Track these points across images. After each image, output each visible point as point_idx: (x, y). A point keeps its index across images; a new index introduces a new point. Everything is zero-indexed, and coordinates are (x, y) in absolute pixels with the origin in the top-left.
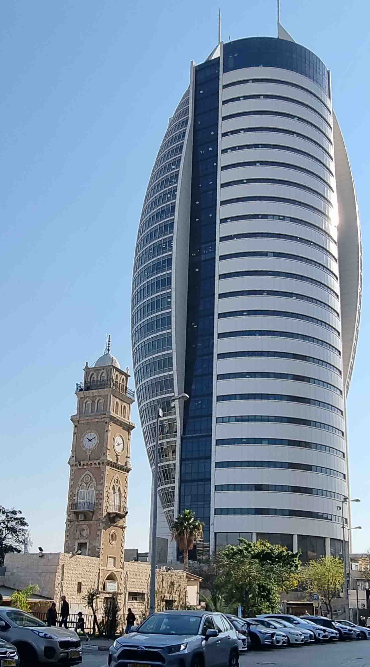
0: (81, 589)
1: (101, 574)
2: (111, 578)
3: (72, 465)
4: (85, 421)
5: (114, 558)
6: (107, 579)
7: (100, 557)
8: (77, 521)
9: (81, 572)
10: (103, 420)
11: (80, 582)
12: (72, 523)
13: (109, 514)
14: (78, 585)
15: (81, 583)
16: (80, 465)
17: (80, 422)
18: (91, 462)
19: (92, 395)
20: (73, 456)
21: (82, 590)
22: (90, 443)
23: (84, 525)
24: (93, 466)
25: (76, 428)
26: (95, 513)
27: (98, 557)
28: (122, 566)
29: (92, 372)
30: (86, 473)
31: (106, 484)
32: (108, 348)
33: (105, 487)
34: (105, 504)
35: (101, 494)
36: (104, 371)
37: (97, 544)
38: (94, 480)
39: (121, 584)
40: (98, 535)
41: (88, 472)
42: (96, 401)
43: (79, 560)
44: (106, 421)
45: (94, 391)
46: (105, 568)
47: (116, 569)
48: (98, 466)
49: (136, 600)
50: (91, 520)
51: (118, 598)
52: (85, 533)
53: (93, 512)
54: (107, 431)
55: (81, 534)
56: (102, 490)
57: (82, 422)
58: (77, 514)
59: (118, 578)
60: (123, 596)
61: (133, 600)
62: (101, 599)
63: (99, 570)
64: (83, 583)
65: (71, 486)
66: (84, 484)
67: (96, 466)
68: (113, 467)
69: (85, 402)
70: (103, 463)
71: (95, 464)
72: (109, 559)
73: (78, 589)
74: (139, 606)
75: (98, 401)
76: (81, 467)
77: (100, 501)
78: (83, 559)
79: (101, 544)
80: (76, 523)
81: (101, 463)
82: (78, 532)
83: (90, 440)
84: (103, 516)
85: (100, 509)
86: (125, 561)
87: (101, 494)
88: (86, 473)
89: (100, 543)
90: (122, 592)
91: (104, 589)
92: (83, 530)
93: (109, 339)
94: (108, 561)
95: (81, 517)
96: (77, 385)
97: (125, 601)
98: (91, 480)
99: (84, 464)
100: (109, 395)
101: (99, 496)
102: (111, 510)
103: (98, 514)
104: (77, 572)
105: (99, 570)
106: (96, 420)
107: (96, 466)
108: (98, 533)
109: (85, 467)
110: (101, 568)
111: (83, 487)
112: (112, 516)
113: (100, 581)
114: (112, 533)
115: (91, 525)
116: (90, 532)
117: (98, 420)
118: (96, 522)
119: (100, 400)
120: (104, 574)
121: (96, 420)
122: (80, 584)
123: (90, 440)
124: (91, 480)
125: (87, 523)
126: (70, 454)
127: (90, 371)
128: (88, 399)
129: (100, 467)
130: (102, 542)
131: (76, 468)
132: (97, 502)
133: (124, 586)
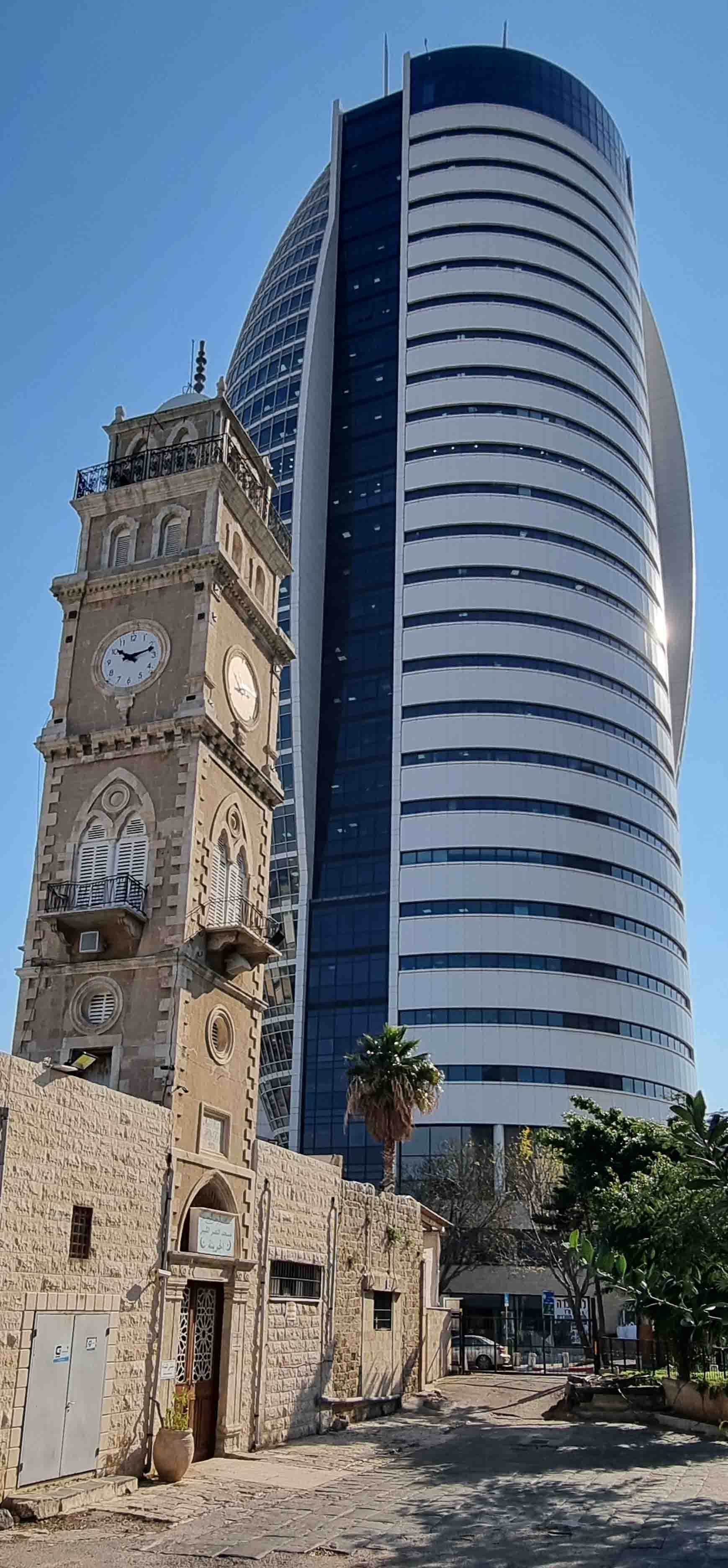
0: (87, 1240)
1: (177, 1180)
2: (212, 1198)
3: (53, 753)
4: (109, 595)
5: (224, 1120)
6: (195, 1203)
7: (175, 1104)
8: (72, 963)
9: (90, 1160)
10: (185, 578)
11: (87, 1204)
12: (48, 973)
13: (207, 935)
14: (75, 1219)
15: (89, 1211)
16: (87, 750)
17: (90, 599)
18: (136, 734)
19: (138, 503)
20: (60, 721)
21: (94, 1242)
22: (129, 665)
23: (102, 976)
24: (145, 748)
25: (73, 624)
26: (150, 926)
27: (164, 1101)
28: (248, 1157)
29: (138, 436)
30: (112, 776)
31: (198, 813)
32: (194, 382)
33: (195, 824)
34: (193, 891)
35: (178, 848)
36: (189, 424)
37: (160, 1052)
38: (146, 798)
39: (247, 1227)
40: (166, 1013)
41: (120, 772)
42: (157, 522)
43: (80, 1099)
44: (198, 581)
45: (149, 484)
46: (192, 1156)
47: (230, 1167)
48: (165, 745)
49: (293, 1293)
50: (134, 956)
51: (238, 1285)
52: (102, 1011)
53: (141, 924)
54: (201, 616)
55: (84, 1014)
56: (182, 834)
57: (99, 597)
58: (69, 931)
59: (238, 1201)
60: (252, 1276)
61: (281, 1293)
62: (175, 1287)
63: (169, 1159)
64: (97, 1213)
65: (47, 831)
66: (103, 822)
67: (156, 748)
68: (224, 757)
69: (111, 528)
70: (186, 732)
71: (152, 738)
72: (203, 1118)
73: (73, 1238)
74: (303, 1318)
75: (165, 522)
76: (91, 758)
77: (173, 879)
78: (102, 1101)
79: (178, 1053)
80: (67, 971)
81: (178, 731)
82: (74, 1009)
83: (132, 658)
84: (187, 938)
85: (173, 907)
86: (257, 1137)
87: (178, 848)
88: (112, 776)
89: (173, 1042)
90: (249, 1259)
91: (185, 1247)
92: (96, 998)
93: (202, 353)
94: (203, 1127)
95: (89, 943)
96: (80, 476)
97: (261, 1296)
98: (134, 799)
99: (101, 746)
100: (211, 494)
101: (170, 857)
102: (214, 920)
103: (163, 932)
104: (72, 1159)
105: (169, 1159)
106: (157, 584)
107: (156, 748)
108: (165, 1004)
109: (109, 755)
110: (177, 1153)
111: (98, 833)
112: (218, 945)
113: (171, 1210)
114: (215, 1016)
115: (131, 974)
116: (127, 1007)
117: (166, 582)
118: (152, 962)
119: (173, 516)
120: (186, 1178)
121: (157, 584)
122: (83, 1217)
123: (132, 658)
124: (134, 799)
125: (115, 966)
126: (47, 714)
127: (134, 432)
128: (122, 519)
129: (169, 750)
130: (179, 1043)
131: (70, 762)
132: (159, 881)
133: (258, 1236)
